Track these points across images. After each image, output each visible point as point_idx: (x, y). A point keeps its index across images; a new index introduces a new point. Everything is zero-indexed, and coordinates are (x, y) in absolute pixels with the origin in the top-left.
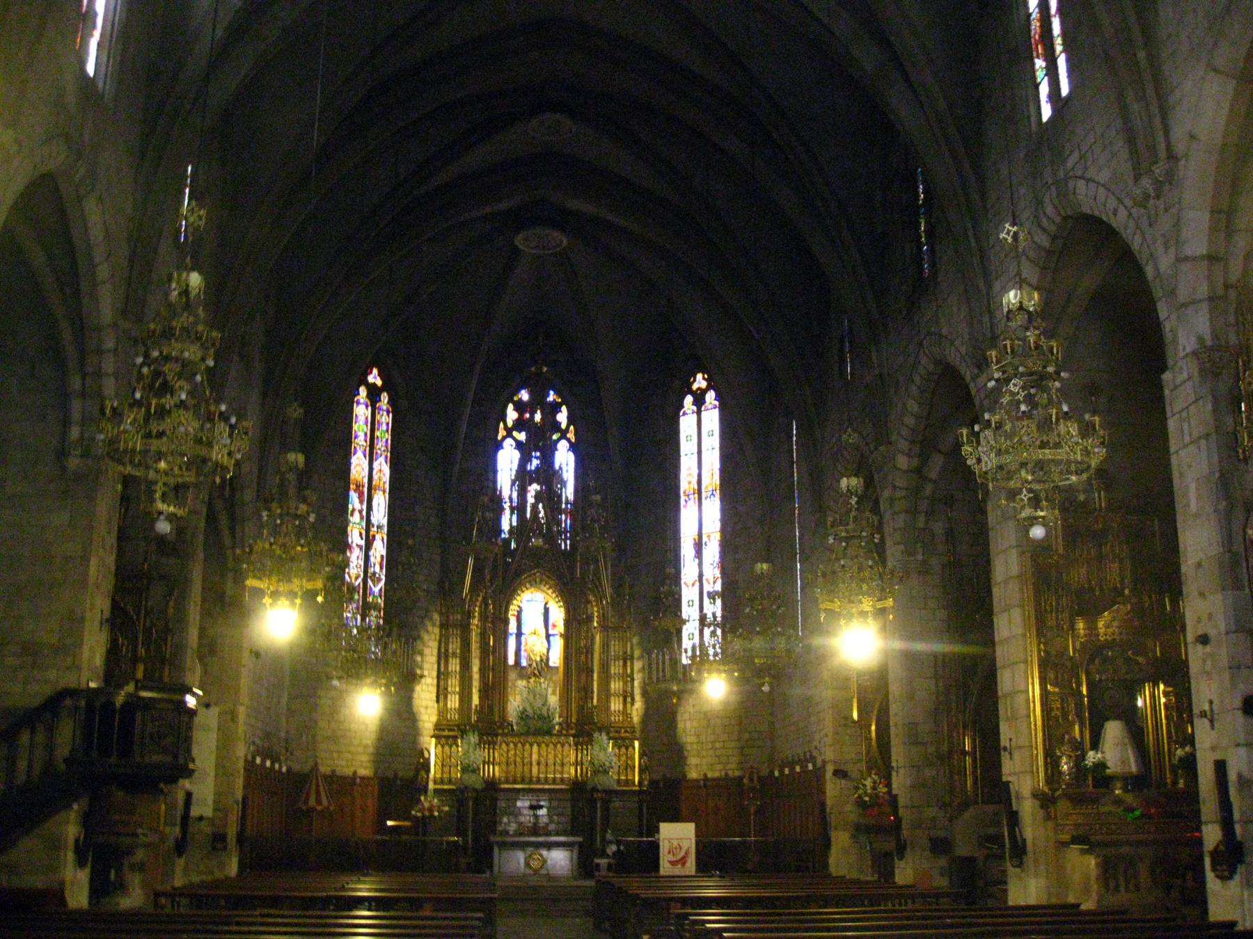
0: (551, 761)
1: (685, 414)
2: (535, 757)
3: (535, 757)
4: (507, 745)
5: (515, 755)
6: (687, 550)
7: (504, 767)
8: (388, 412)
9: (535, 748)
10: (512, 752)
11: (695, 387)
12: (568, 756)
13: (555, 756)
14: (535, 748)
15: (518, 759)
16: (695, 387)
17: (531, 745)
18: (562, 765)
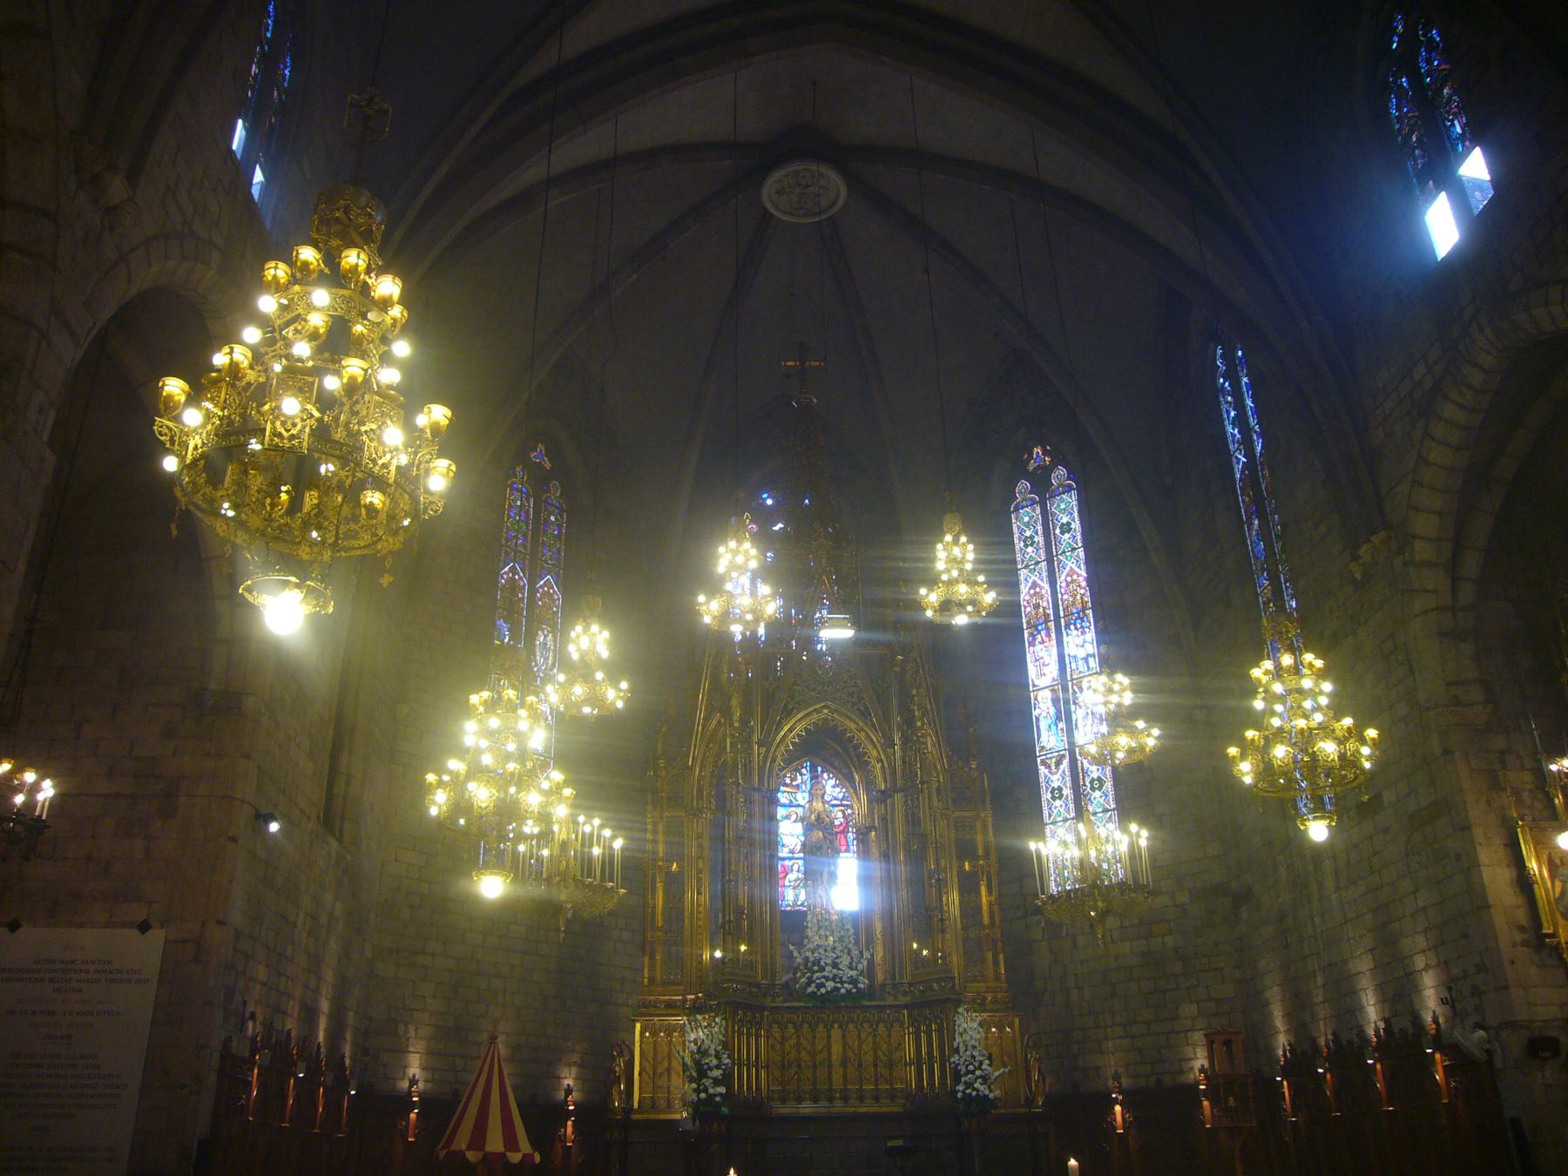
0: (869, 1059)
1: (1017, 510)
2: (836, 1049)
3: (836, 1049)
4: (782, 1027)
5: (798, 1045)
6: (1043, 707)
7: (777, 1074)
8: (561, 510)
9: (836, 1032)
10: (793, 1041)
11: (1032, 466)
12: (900, 1046)
13: (875, 1047)
14: (836, 1032)
15: (804, 1056)
16: (1032, 466)
17: (829, 1028)
18: (890, 1065)
